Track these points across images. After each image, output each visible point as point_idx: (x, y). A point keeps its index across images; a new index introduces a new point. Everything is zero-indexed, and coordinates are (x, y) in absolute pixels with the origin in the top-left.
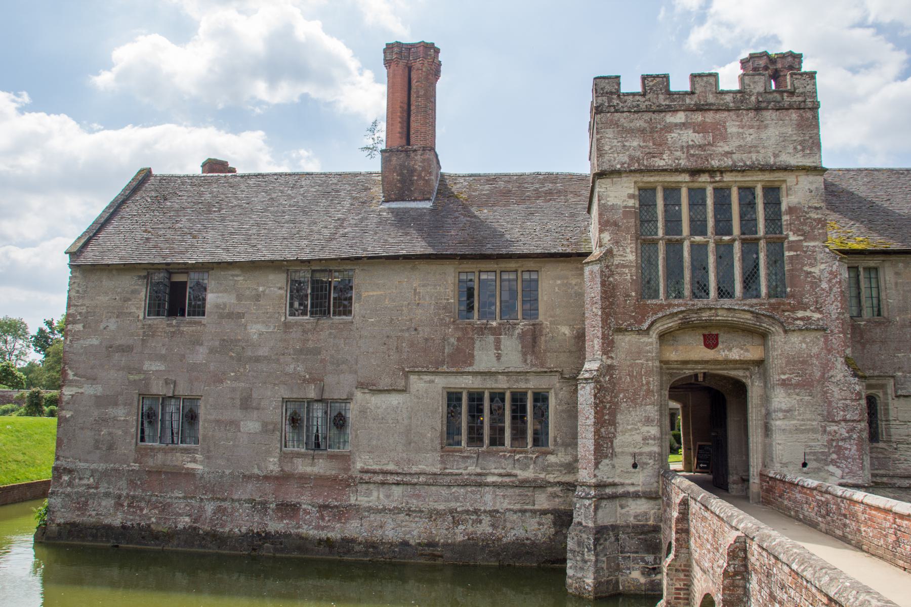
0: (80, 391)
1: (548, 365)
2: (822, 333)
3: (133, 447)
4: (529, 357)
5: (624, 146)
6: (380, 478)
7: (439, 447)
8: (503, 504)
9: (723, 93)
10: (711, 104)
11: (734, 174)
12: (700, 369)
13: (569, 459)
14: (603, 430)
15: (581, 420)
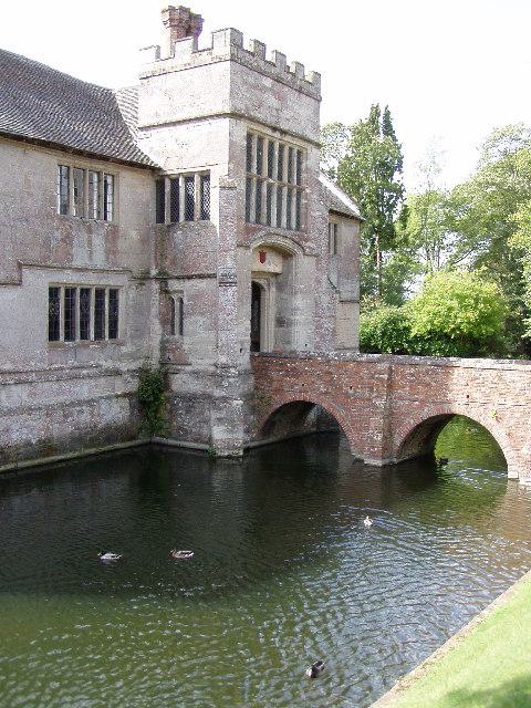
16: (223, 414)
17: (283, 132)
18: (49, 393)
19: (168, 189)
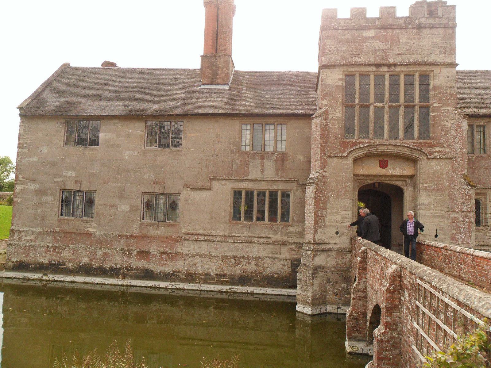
0: (27, 187)
1: (290, 177)
2: (450, 160)
3: (56, 219)
4: (279, 172)
5: (338, 50)
6: (195, 238)
7: (228, 221)
8: (263, 254)
9: (399, 18)
10: (391, 25)
11: (403, 67)
12: (376, 180)
13: (301, 229)
14: (319, 212)
15: (307, 206)
18: (226, 250)
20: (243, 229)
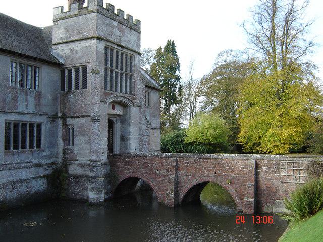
16: (94, 185)
17: (123, 47)
19: (66, 74)
20: (14, 158)
